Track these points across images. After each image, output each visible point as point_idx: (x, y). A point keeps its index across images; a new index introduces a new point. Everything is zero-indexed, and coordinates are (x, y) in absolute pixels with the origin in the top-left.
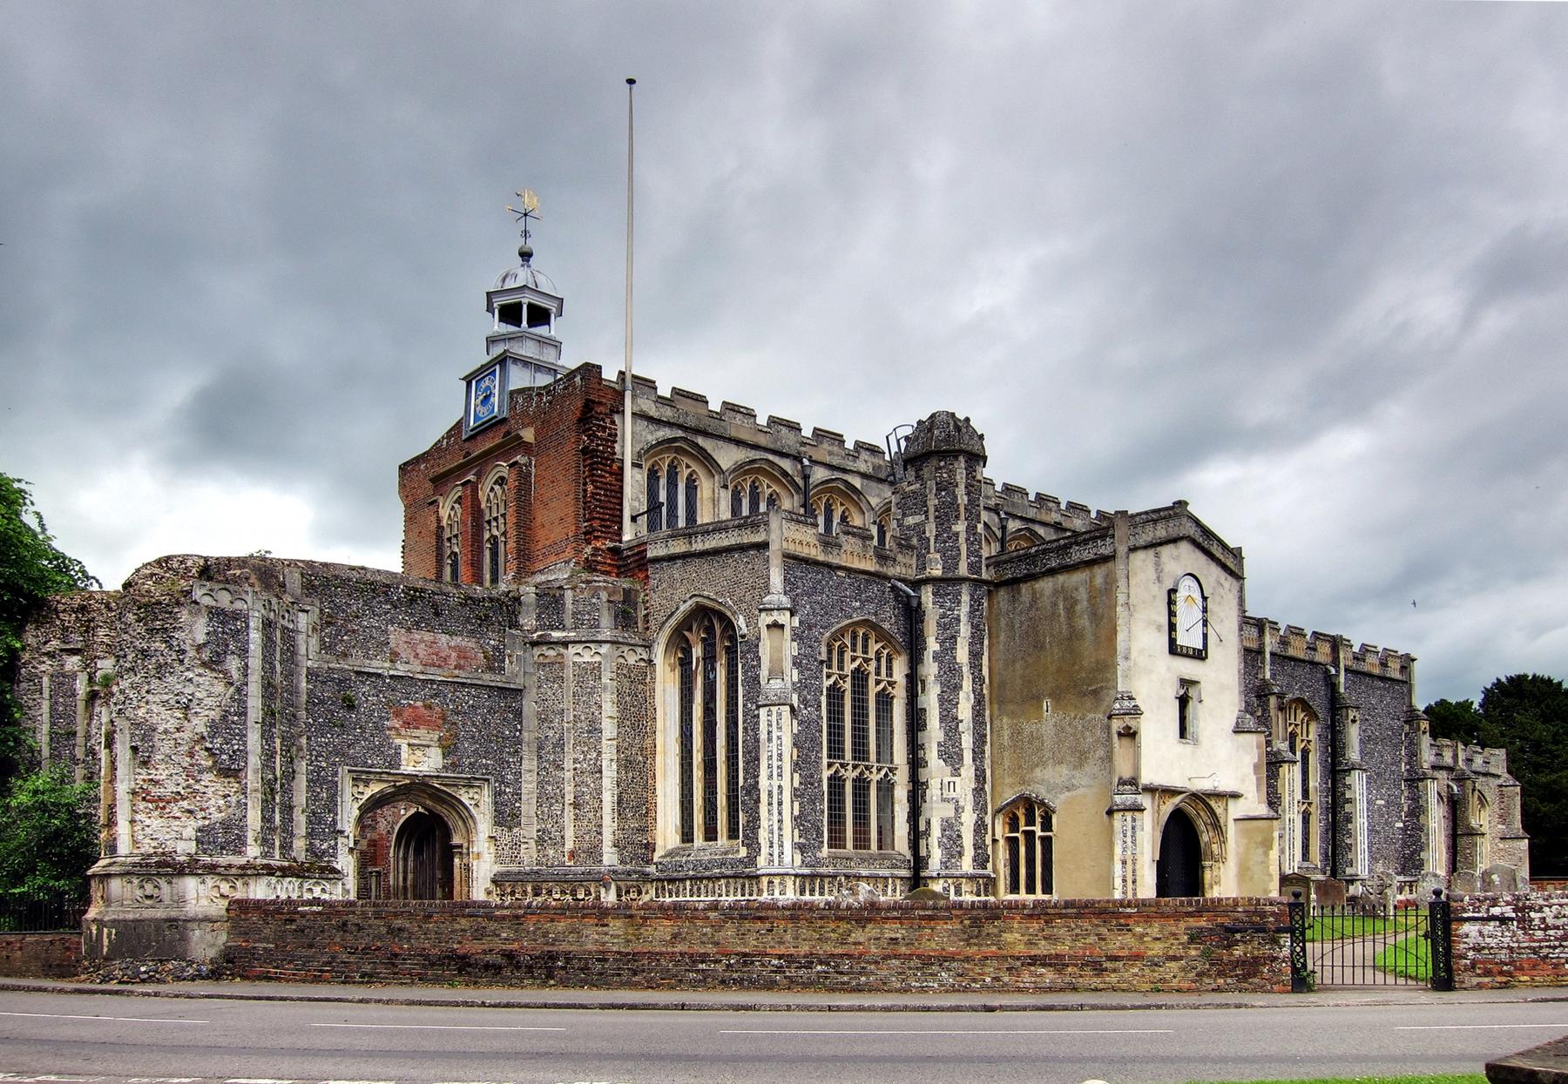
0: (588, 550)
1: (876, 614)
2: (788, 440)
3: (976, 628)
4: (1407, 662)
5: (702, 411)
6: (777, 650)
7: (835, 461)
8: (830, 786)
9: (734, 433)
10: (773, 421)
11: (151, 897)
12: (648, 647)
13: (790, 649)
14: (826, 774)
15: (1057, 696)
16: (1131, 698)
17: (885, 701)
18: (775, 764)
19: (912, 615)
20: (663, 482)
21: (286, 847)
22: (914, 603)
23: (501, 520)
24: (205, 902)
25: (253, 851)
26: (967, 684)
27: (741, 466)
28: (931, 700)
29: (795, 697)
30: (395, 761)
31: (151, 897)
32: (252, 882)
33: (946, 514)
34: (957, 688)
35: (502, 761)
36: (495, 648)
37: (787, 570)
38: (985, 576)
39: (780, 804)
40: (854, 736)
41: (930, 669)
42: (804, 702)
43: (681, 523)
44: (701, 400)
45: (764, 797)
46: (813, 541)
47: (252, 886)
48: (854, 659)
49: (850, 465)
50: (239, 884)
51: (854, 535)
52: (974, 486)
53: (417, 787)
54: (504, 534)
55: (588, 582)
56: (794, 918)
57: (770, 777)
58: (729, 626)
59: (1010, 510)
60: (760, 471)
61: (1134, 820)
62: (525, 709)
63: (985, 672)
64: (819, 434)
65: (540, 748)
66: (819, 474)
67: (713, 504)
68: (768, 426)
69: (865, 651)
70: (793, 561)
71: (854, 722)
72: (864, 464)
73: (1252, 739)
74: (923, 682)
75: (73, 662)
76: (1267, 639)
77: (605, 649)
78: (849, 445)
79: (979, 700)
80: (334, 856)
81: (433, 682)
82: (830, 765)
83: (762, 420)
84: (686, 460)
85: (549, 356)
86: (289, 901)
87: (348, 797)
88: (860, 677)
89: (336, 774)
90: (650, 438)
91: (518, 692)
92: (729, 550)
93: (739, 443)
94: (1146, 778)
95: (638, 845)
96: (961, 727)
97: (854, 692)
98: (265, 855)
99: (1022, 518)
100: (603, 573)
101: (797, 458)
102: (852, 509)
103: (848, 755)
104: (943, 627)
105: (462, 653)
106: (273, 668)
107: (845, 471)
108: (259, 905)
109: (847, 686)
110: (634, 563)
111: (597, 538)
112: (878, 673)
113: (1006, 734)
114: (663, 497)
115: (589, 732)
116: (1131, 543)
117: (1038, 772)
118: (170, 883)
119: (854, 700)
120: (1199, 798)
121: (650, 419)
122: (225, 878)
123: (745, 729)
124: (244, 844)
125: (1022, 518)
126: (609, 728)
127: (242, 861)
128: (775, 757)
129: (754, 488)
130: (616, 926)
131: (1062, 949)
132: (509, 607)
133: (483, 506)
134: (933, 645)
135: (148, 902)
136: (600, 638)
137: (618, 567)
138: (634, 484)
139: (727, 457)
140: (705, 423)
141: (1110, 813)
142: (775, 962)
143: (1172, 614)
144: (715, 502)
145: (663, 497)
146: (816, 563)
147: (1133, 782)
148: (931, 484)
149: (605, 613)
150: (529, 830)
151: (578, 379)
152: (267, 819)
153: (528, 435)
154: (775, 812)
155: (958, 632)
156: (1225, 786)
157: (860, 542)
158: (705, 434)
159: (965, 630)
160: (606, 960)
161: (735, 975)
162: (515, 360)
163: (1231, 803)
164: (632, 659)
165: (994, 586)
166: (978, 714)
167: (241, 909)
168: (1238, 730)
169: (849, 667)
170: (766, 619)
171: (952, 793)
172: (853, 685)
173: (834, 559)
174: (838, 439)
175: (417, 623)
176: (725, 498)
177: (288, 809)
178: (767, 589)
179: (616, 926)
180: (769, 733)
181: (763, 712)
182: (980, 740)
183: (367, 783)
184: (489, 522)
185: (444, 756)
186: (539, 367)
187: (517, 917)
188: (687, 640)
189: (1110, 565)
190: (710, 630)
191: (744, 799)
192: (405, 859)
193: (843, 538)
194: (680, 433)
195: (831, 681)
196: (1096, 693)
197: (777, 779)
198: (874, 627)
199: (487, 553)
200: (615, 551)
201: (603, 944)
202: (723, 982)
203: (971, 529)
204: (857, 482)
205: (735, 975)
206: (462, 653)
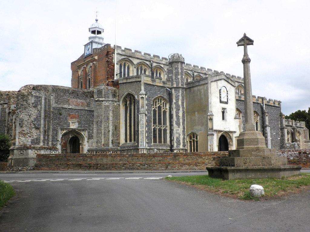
0: (108, 82)
1: (163, 95)
2: (148, 57)
3: (183, 97)
4: (279, 103)
5: (130, 52)
6: (143, 103)
7: (158, 62)
8: (153, 130)
9: (137, 57)
10: (145, 54)
11: (22, 154)
12: (119, 101)
13: (146, 102)
14: (153, 128)
15: (198, 111)
16: (211, 112)
17: (165, 112)
19: (170, 94)
20: (123, 67)
21: (48, 143)
22: (171, 92)
23: (91, 75)
24: (32, 155)
25: (42, 144)
26: (181, 109)
27: (138, 63)
28: (174, 112)
29: (146, 112)
30: (69, 126)
31: (22, 154)
32: (41, 150)
34: (179, 110)
35: (90, 125)
36: (89, 102)
37: (145, 86)
38: (185, 86)
39: (143, 134)
40: (158, 120)
41: (174, 106)
42: (148, 113)
43: (126, 76)
44: (130, 50)
45: (140, 132)
46: (150, 80)
47: (41, 152)
48: (158, 104)
49: (161, 62)
50: (39, 151)
51: (158, 79)
52: (182, 69)
53: (73, 131)
54: (91, 78)
55: (107, 88)
56: (142, 156)
57: (141, 128)
58: (134, 97)
59: (195, 71)
60: (142, 64)
61: (212, 137)
62: (95, 115)
63: (185, 106)
64: (154, 56)
66: (154, 64)
67: (133, 72)
68: (144, 55)
69: (161, 102)
70: (146, 84)
71: (158, 117)
72: (164, 62)
73: (238, 120)
74: (172, 108)
75: (5, 106)
77: (110, 102)
78: (161, 58)
79: (184, 112)
80: (57, 145)
81: (76, 109)
82: (153, 126)
83: (143, 54)
84: (127, 62)
85: (101, 41)
86: (48, 154)
87: (60, 133)
88: (160, 108)
89: (57, 128)
90: (120, 58)
91: (93, 111)
92: (134, 82)
93: (138, 58)
94: (215, 128)
95: (116, 142)
97: (158, 111)
98: (44, 145)
99: (197, 72)
100: (110, 86)
101: (150, 61)
102: (162, 71)
103: (157, 124)
104: (176, 97)
105: (82, 103)
107: (160, 63)
108: (43, 155)
109: (157, 109)
110: (116, 84)
111: (109, 79)
112: (163, 107)
113: (189, 119)
114: (123, 71)
115: (107, 119)
117: (195, 127)
118: (25, 151)
119: (158, 112)
120: (226, 132)
121: (120, 54)
122: (36, 150)
123: (137, 118)
124: (40, 143)
125: (197, 72)
126: (111, 118)
127: (40, 146)
129: (141, 67)
130: (109, 158)
131: (190, 162)
132: (92, 95)
133: (87, 72)
134: (174, 101)
135: (21, 155)
136: (109, 100)
137: (113, 85)
138: (117, 67)
139: (136, 62)
140: (131, 55)
141: (208, 135)
142: (138, 165)
144: (133, 71)
145: (123, 71)
146: (151, 85)
147: (212, 129)
150: (95, 140)
151: (106, 47)
152: (44, 138)
153: (96, 58)
155: (179, 98)
156: (232, 130)
157: (159, 80)
158: (131, 57)
159: (180, 98)
160: (107, 165)
161: (131, 167)
162: (94, 42)
163: (234, 133)
165: (186, 89)
166: (183, 115)
167: (39, 156)
168: (235, 118)
169: (158, 105)
170: (140, 96)
171: (178, 131)
172: (158, 109)
173: (154, 84)
174: (158, 57)
175: (74, 97)
176: (135, 70)
177: (48, 136)
178: (141, 90)
179: (109, 158)
180: (141, 119)
181: (140, 115)
182: (184, 120)
183: (63, 130)
184: (88, 75)
185: (79, 124)
186: (99, 43)
187: (91, 157)
188: (126, 100)
189: (207, 85)
190: (131, 98)
191: (136, 133)
192: (70, 146)
193: (156, 79)
194: (126, 57)
195: (154, 108)
196: (205, 111)
197: (143, 129)
198: (162, 97)
199: (88, 82)
200: (113, 82)
201: (107, 161)
202: (129, 169)
203: (182, 77)
204: (162, 66)
205: (131, 167)
206: (82, 103)
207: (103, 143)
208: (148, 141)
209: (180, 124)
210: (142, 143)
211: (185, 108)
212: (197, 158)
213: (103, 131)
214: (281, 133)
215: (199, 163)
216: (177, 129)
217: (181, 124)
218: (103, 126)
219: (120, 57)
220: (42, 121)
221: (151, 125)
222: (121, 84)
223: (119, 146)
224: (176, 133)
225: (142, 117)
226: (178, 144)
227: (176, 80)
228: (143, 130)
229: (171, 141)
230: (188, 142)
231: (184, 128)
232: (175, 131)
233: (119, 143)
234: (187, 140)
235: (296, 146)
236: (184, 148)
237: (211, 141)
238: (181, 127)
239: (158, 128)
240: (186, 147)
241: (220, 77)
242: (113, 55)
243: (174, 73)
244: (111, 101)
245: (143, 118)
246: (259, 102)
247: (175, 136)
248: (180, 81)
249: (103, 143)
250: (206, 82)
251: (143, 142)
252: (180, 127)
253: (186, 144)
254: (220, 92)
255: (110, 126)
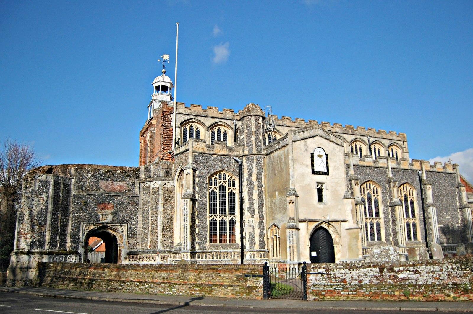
9: (210, 115)
17: (232, 195)
18: (186, 217)
28: (245, 194)
33: (249, 135)
34: (253, 189)
38: (263, 152)
41: (245, 183)
63: (263, 184)
65: (143, 213)
76: (390, 163)
79: (261, 193)
80: (78, 248)
88: (222, 189)
93: (212, 117)
94: (302, 217)
96: (254, 202)
106: (59, 195)
109: (217, 191)
115: (155, 208)
116: (293, 140)
124: (44, 246)
128: (186, 215)
134: (246, 176)
142: (137, 284)
143: (312, 161)
148: (245, 126)
149: (161, 172)
154: (185, 232)
155: (253, 171)
159: (255, 171)
164: (169, 185)
166: (260, 198)
169: (218, 185)
171: (251, 222)
180: (184, 207)
182: (261, 205)
185: (113, 217)
194: (192, 117)
203: (257, 139)
207: (149, 243)
208: (199, 241)
209: (254, 211)
210: (185, 243)
211: (264, 186)
212: (213, 275)
213: (150, 225)
214: (461, 215)
215: (215, 285)
216: (250, 219)
217: (256, 211)
218: (150, 218)
219: (183, 118)
220: (49, 216)
221: (205, 216)
222: (177, 154)
223: (172, 248)
224: (249, 226)
225: (186, 204)
226: (253, 243)
227: (249, 143)
228: (187, 224)
229: (242, 238)
230: (270, 239)
231: (261, 218)
232: (246, 224)
233: (173, 243)
234: (267, 237)
235: (390, 252)
236: (262, 250)
237: (291, 239)
238: (257, 215)
239: (218, 219)
240: (266, 248)
241: (312, 133)
242: (171, 116)
243: (245, 134)
244: (161, 182)
245: (187, 206)
246: (414, 168)
247: (247, 231)
248: (254, 144)
249: (149, 243)
250: (286, 143)
251: (187, 243)
252: (255, 216)
253: (266, 243)
254: (312, 157)
255: (159, 217)
